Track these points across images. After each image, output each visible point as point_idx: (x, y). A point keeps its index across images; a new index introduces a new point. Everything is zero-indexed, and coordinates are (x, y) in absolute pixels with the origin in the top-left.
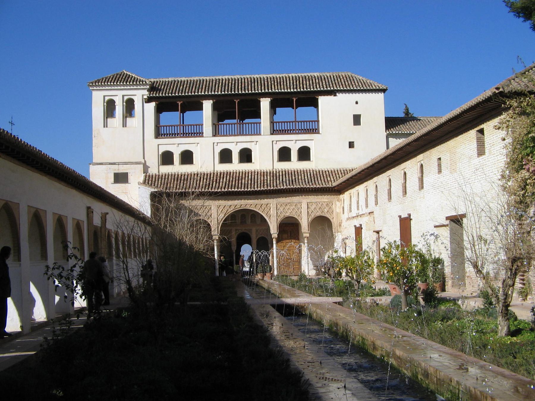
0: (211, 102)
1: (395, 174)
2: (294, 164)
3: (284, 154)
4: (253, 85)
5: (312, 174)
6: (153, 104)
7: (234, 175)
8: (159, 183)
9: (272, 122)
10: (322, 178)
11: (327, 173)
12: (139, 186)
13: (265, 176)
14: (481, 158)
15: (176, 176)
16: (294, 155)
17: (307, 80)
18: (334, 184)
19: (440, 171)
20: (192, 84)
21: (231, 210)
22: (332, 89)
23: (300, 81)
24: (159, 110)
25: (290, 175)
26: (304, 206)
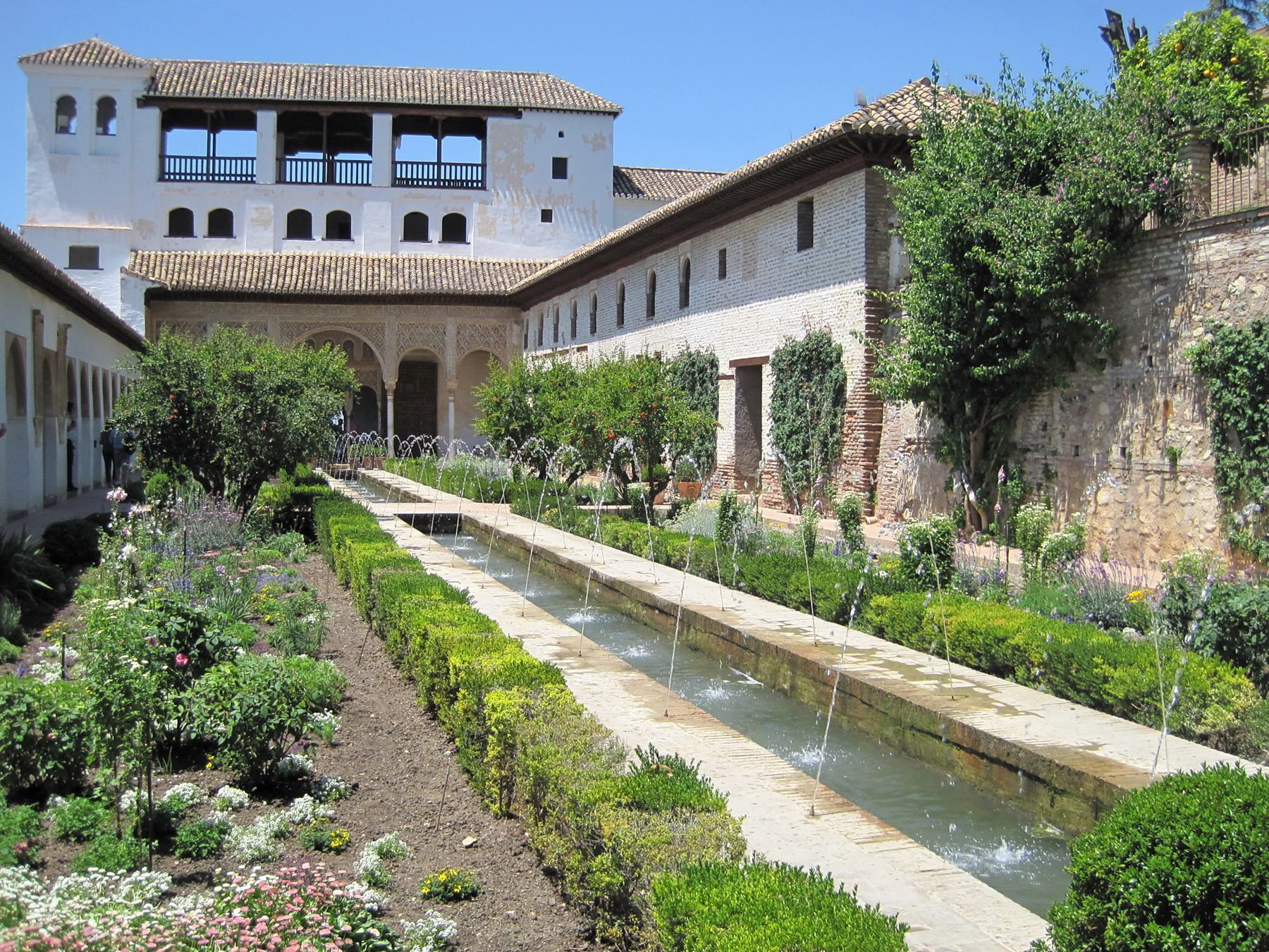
3: (415, 228)
4: (359, 86)
14: (805, 252)
19: (723, 275)
26: (451, 330)
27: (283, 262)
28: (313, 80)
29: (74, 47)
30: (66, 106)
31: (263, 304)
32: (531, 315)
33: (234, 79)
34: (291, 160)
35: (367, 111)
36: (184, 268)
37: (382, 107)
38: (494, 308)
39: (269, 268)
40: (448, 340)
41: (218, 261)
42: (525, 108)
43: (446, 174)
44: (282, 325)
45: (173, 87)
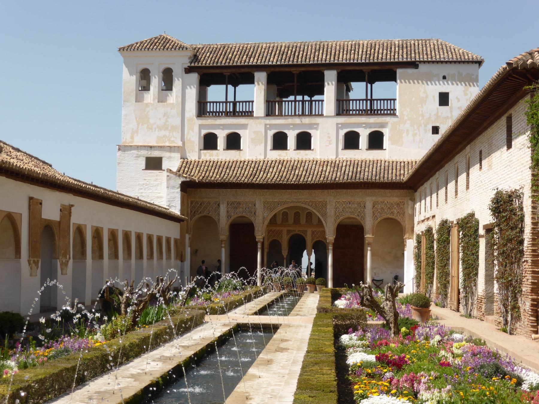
3: (351, 141)
4: (317, 53)
5: (383, 165)
6: (194, 77)
7: (288, 165)
8: (197, 171)
10: (394, 171)
11: (402, 164)
12: (168, 174)
13: (325, 167)
15: (219, 163)
17: (385, 48)
18: (405, 178)
20: (243, 51)
22: (413, 60)
23: (375, 50)
25: (356, 166)
26: (369, 205)
27: (269, 164)
28: (289, 52)
29: (151, 40)
31: (253, 190)
33: (243, 52)
34: (285, 101)
35: (321, 68)
36: (209, 169)
37: (330, 66)
38: (397, 191)
39: (260, 168)
41: (230, 164)
42: (420, 62)
44: (264, 203)
45: (206, 61)
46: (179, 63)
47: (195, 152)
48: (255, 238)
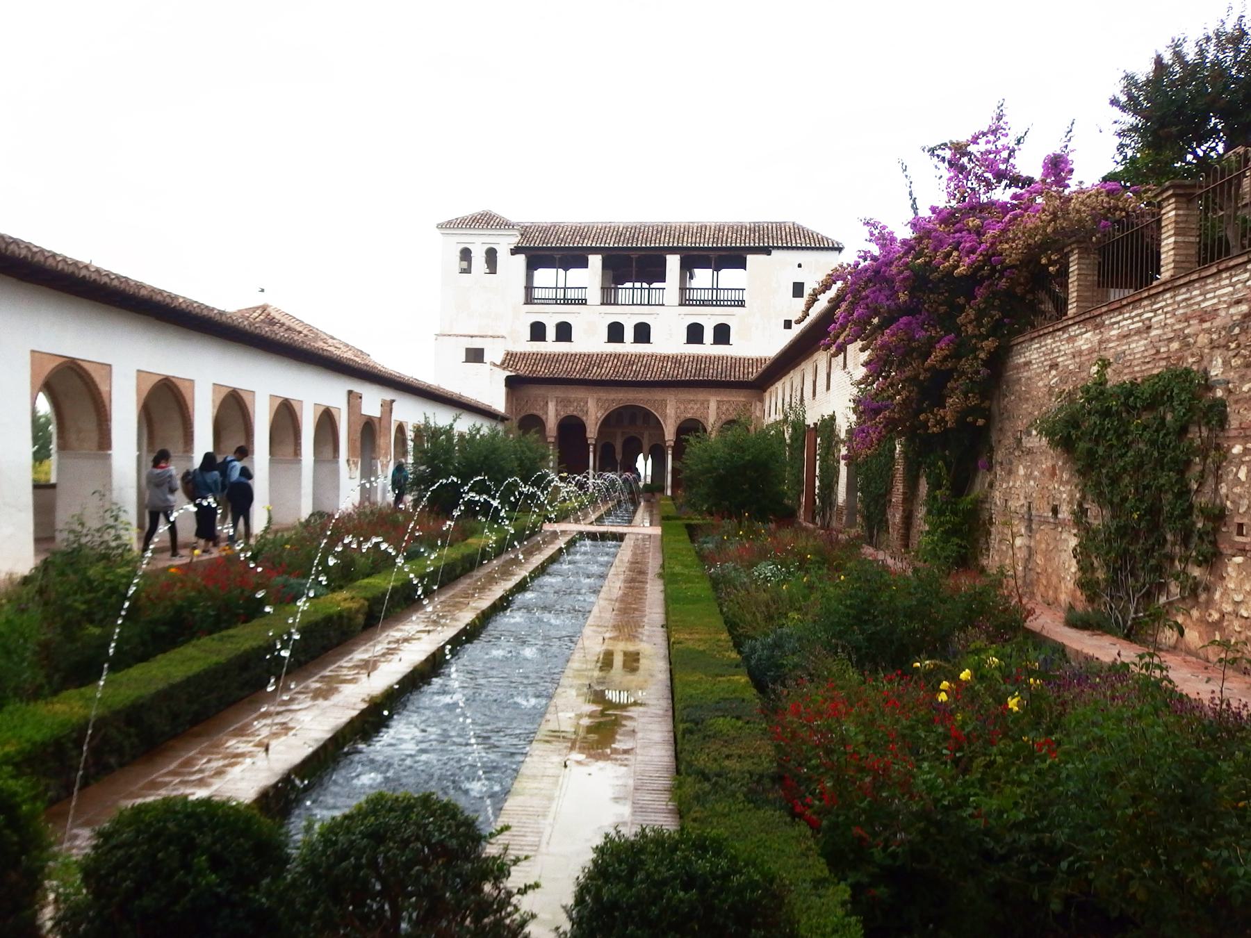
0: (599, 257)
1: (807, 367)
2: (708, 348)
3: (695, 333)
6: (521, 259)
9: (683, 289)
16: (708, 335)
21: (614, 406)
24: (532, 266)
26: (713, 405)
30: (466, 254)
32: (767, 394)
40: (712, 410)
42: (774, 248)
43: (722, 295)
46: (504, 243)
47: (523, 344)
48: (586, 440)
